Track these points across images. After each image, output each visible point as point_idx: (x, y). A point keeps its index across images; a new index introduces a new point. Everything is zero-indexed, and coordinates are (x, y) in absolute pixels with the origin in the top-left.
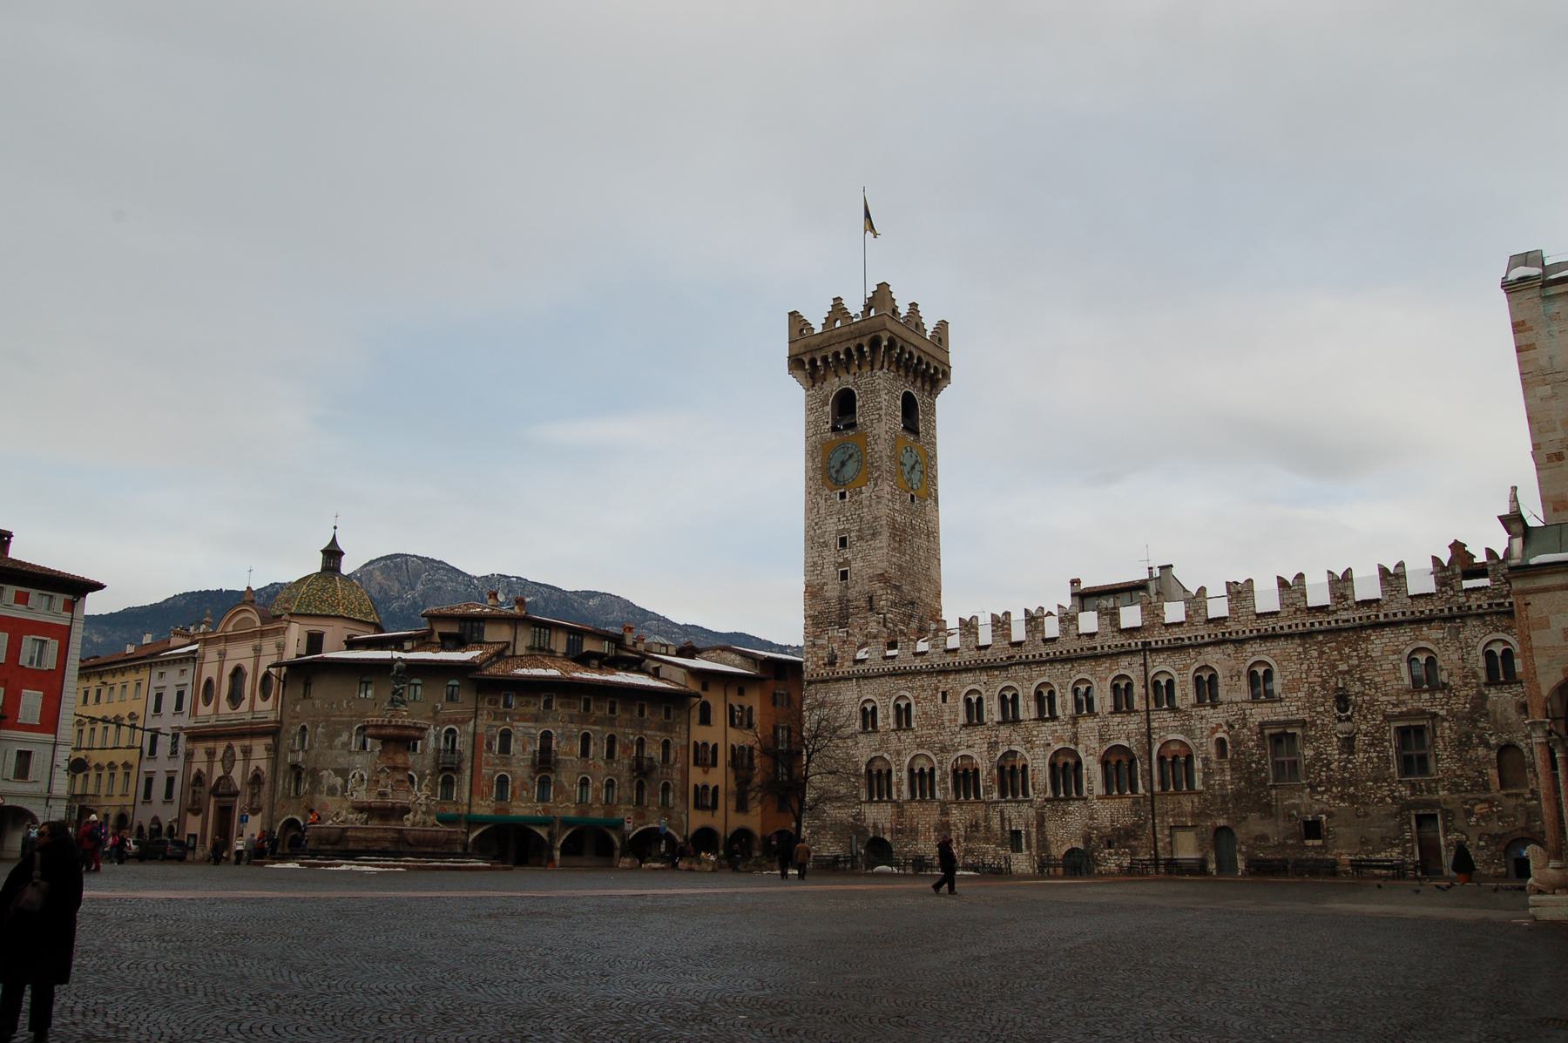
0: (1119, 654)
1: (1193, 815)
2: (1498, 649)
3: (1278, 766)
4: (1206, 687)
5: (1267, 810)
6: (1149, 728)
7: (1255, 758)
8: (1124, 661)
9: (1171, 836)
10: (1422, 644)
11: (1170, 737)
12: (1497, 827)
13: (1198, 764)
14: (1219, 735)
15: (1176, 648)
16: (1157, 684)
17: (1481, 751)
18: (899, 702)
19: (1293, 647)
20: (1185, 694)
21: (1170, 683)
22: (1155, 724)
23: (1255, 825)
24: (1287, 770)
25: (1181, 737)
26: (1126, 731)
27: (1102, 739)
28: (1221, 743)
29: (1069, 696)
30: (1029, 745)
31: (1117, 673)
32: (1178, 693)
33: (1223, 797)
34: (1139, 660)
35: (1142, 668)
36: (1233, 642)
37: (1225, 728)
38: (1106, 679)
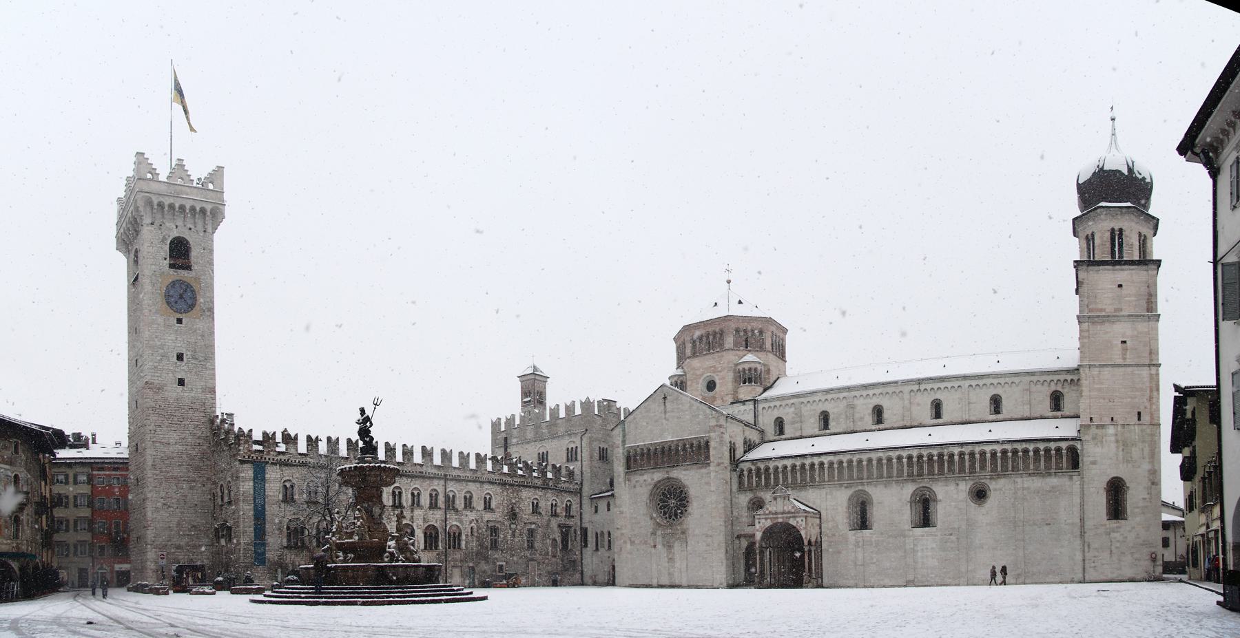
0: (433, 478)
1: (461, 561)
2: (554, 503)
3: (491, 539)
4: (468, 503)
5: (486, 559)
6: (446, 518)
7: (485, 536)
8: (436, 482)
9: (451, 570)
10: (537, 497)
11: (454, 523)
12: (549, 569)
13: (464, 537)
14: (473, 524)
15: (457, 479)
16: (449, 498)
17: (548, 540)
18: (286, 484)
19: (498, 489)
20: (460, 504)
21: (454, 497)
22: (448, 516)
23: (484, 566)
24: (494, 545)
25: (458, 524)
26: (436, 518)
27: (425, 520)
28: (472, 528)
29: (410, 496)
30: (388, 520)
31: (432, 488)
32: (457, 502)
33: (473, 553)
34: (442, 482)
35: (444, 487)
36: (480, 482)
37: (475, 522)
38: (427, 490)
